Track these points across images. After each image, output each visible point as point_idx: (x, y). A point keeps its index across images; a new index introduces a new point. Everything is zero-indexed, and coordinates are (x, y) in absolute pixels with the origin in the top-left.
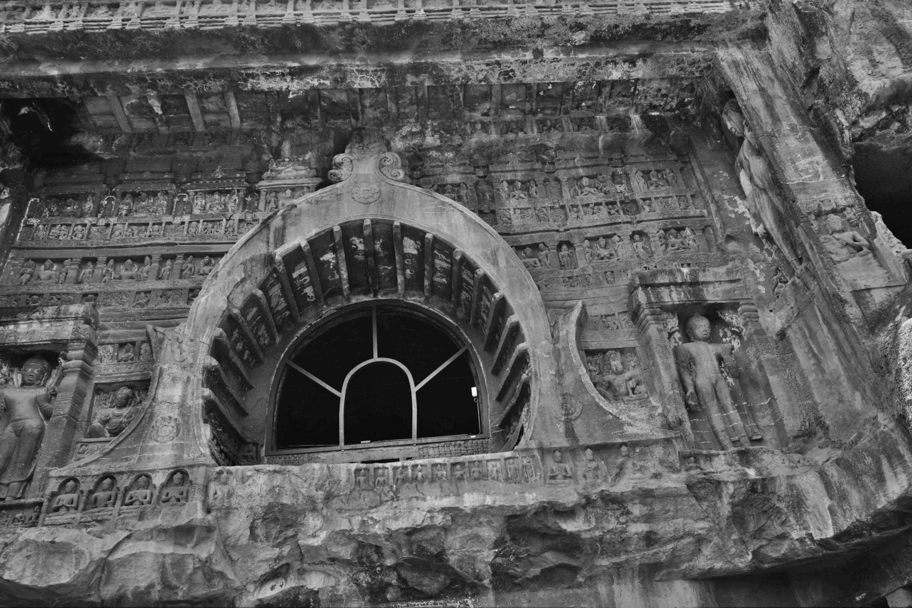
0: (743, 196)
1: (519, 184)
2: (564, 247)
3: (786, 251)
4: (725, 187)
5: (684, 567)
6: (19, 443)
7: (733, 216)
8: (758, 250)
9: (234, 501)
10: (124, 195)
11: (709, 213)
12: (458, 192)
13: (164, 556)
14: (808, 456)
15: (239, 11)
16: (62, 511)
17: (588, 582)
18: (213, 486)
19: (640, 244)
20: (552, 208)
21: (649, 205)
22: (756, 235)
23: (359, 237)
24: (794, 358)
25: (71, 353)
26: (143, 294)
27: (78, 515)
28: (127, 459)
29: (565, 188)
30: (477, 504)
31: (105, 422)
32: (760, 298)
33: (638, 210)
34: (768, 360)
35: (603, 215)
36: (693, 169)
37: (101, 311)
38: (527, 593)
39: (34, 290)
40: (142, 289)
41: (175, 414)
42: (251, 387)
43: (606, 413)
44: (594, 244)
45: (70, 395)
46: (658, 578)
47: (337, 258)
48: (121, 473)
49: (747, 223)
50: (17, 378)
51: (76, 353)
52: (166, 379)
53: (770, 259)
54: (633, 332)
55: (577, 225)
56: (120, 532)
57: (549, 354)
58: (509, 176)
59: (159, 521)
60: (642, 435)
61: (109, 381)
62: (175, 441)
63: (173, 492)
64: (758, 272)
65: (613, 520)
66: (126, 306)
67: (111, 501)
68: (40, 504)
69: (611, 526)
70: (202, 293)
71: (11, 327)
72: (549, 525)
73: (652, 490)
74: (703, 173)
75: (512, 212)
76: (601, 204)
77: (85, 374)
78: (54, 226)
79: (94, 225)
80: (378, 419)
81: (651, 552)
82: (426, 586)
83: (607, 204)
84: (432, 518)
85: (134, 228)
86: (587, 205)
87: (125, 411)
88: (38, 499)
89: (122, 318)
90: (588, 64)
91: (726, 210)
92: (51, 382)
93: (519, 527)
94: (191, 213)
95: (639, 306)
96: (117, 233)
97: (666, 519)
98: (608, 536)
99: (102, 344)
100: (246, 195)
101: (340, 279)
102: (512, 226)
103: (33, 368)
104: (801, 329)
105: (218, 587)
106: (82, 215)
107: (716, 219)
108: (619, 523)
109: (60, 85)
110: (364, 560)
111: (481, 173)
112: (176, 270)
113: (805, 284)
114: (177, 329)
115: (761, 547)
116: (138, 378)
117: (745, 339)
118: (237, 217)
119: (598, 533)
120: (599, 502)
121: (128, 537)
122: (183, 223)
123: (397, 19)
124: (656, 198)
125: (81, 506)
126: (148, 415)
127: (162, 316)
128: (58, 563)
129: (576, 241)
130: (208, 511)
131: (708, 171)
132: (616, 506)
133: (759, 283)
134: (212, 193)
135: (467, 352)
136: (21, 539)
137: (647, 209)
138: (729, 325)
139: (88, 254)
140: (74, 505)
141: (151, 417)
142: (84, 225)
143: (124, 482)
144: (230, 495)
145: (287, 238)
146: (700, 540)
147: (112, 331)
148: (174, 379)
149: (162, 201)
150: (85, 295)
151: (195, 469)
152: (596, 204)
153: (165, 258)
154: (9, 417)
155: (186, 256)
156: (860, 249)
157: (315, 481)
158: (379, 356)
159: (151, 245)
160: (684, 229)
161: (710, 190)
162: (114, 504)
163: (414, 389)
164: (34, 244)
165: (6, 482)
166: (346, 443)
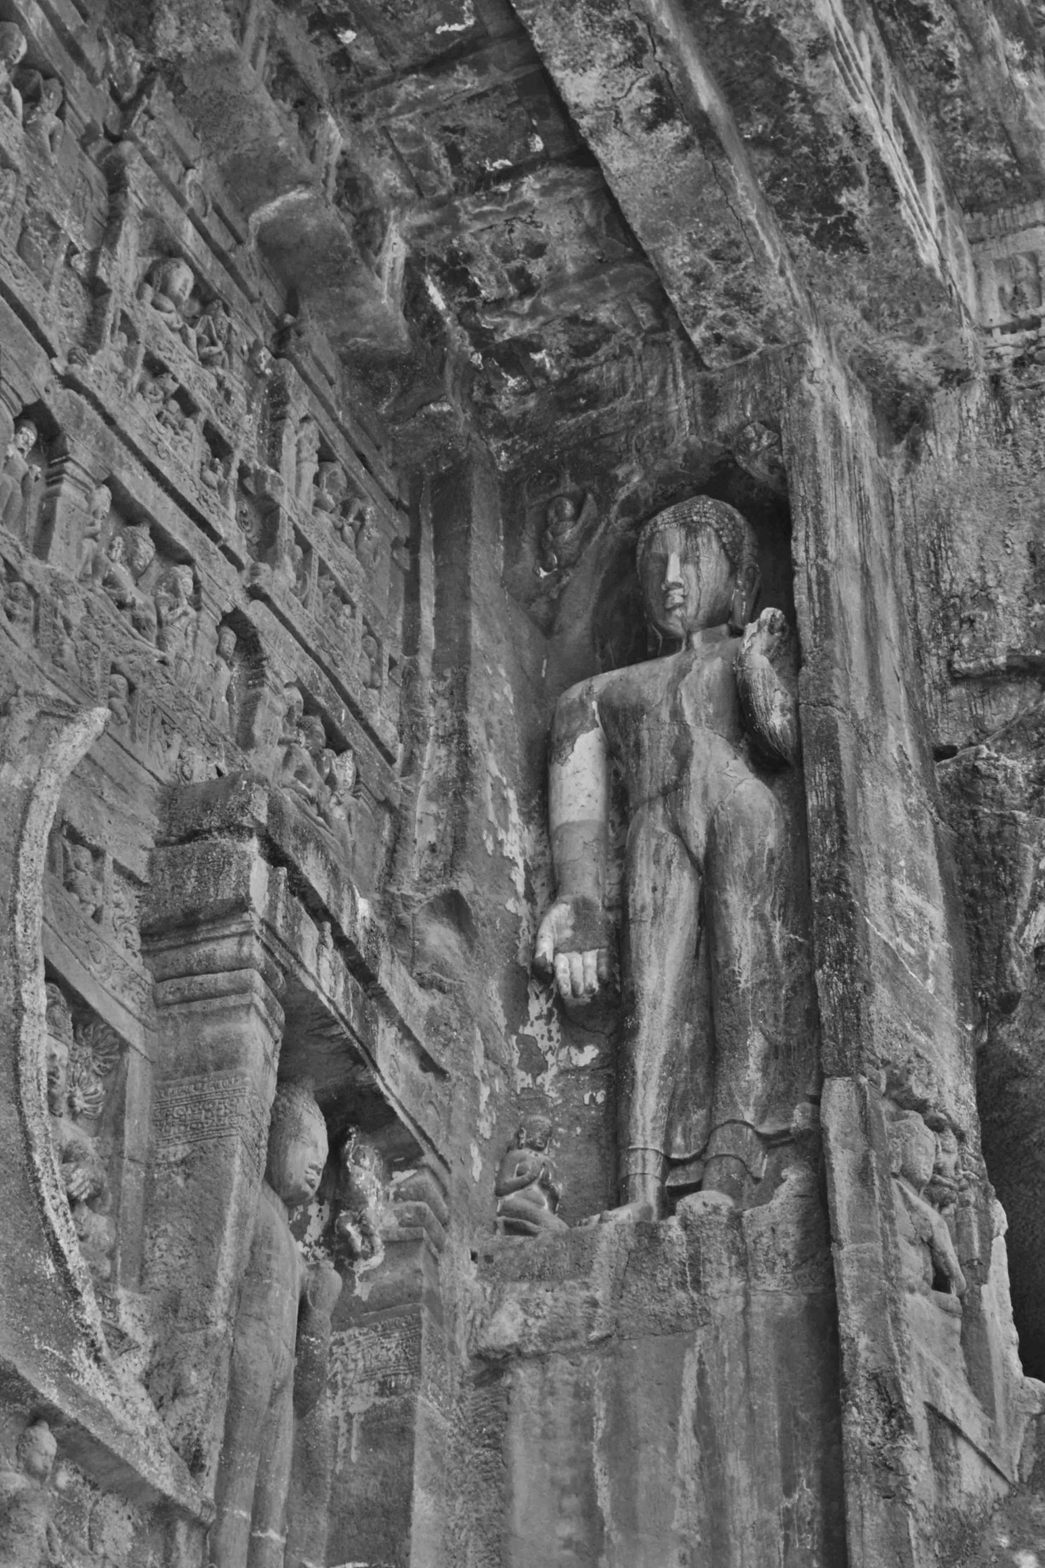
2: (29, 435)
7: (490, 846)
8: (502, 1021)
11: (410, 765)
19: (226, 674)
20: (72, 251)
22: (543, 975)
53: (523, 1079)
60: (119, 1430)
83: (211, 434)
91: (481, 805)
104: (582, 1393)
113: (696, 1261)
117: (362, 1291)
129: (81, 454)
152: (182, 396)
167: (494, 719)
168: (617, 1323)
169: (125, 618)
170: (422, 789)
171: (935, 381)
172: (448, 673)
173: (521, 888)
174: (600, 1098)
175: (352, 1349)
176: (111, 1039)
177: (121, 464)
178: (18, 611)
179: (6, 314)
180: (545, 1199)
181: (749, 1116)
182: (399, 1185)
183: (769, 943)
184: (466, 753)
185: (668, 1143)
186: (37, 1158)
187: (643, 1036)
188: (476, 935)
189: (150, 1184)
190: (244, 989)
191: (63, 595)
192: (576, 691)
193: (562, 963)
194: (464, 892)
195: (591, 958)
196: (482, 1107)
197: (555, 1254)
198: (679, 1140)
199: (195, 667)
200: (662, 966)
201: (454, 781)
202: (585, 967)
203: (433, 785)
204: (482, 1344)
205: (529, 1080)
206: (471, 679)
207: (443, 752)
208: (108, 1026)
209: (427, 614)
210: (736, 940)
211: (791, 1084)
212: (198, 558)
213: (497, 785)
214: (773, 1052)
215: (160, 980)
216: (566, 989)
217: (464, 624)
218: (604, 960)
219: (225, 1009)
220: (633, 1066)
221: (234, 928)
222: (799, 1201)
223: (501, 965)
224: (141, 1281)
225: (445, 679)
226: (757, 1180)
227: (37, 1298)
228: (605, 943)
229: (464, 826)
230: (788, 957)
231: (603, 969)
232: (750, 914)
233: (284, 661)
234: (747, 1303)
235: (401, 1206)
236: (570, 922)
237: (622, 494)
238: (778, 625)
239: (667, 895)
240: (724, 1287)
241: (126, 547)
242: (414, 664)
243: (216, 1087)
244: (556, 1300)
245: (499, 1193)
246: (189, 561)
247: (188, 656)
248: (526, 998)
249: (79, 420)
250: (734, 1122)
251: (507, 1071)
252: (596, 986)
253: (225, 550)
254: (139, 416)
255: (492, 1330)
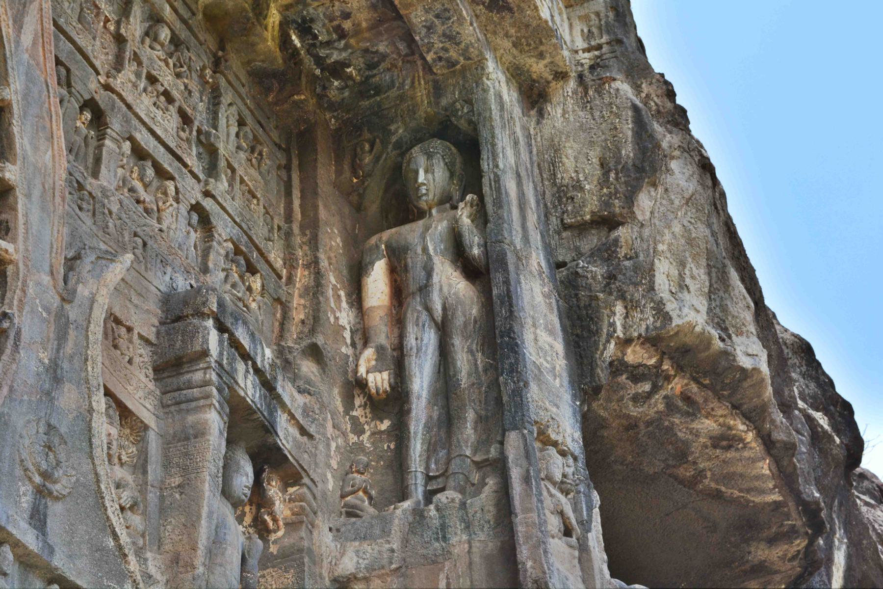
2: (88, 115)
7: (332, 320)
8: (341, 409)
11: (290, 280)
19: (194, 236)
20: (107, 20)
22: (361, 385)
54: (151, 393)
57: (47, 309)
83: (182, 113)
91: (327, 299)
113: (443, 527)
117: (273, 549)
129: (115, 125)
152: (166, 94)
167: (332, 255)
168: (404, 560)
169: (140, 208)
170: (297, 292)
171: (551, 77)
172: (308, 232)
173: (349, 341)
174: (392, 446)
175: (269, 579)
176: (139, 424)
177: (136, 129)
178: (85, 206)
179: (74, 53)
180: (366, 498)
181: (468, 453)
182: (291, 495)
183: (476, 364)
184: (318, 273)
185: (427, 468)
186: (103, 487)
187: (413, 414)
188: (326, 365)
189: (162, 498)
190: (208, 396)
191: (107, 197)
192: (374, 240)
193: (371, 378)
194: (319, 343)
195: (385, 375)
196: (332, 453)
197: (372, 526)
198: (433, 466)
199: (178, 232)
200: (421, 378)
201: (313, 287)
202: (383, 380)
203: (302, 290)
204: (336, 574)
205: (356, 438)
206: (320, 236)
207: (306, 273)
208: (138, 418)
209: (297, 203)
210: (459, 363)
211: (489, 435)
212: (177, 176)
213: (335, 289)
214: (479, 419)
215: (164, 393)
216: (373, 391)
217: (316, 207)
218: (392, 376)
219: (198, 407)
220: (408, 429)
221: (201, 366)
222: (495, 494)
223: (339, 380)
224: (159, 548)
225: (306, 235)
226: (473, 485)
227: (105, 558)
228: (392, 367)
229: (318, 310)
230: (485, 371)
231: (392, 380)
232: (466, 350)
233: (224, 229)
234: (470, 547)
235: (292, 505)
236: (374, 357)
237: (394, 139)
238: (475, 203)
239: (423, 343)
240: (458, 540)
241: (140, 172)
242: (291, 228)
243: (195, 447)
244: (373, 550)
245: (343, 497)
246: (172, 178)
247: (173, 227)
248: (353, 397)
249: (113, 107)
250: (461, 455)
251: (344, 434)
252: (388, 389)
253: (191, 172)
254: (144, 105)
255: (341, 566)
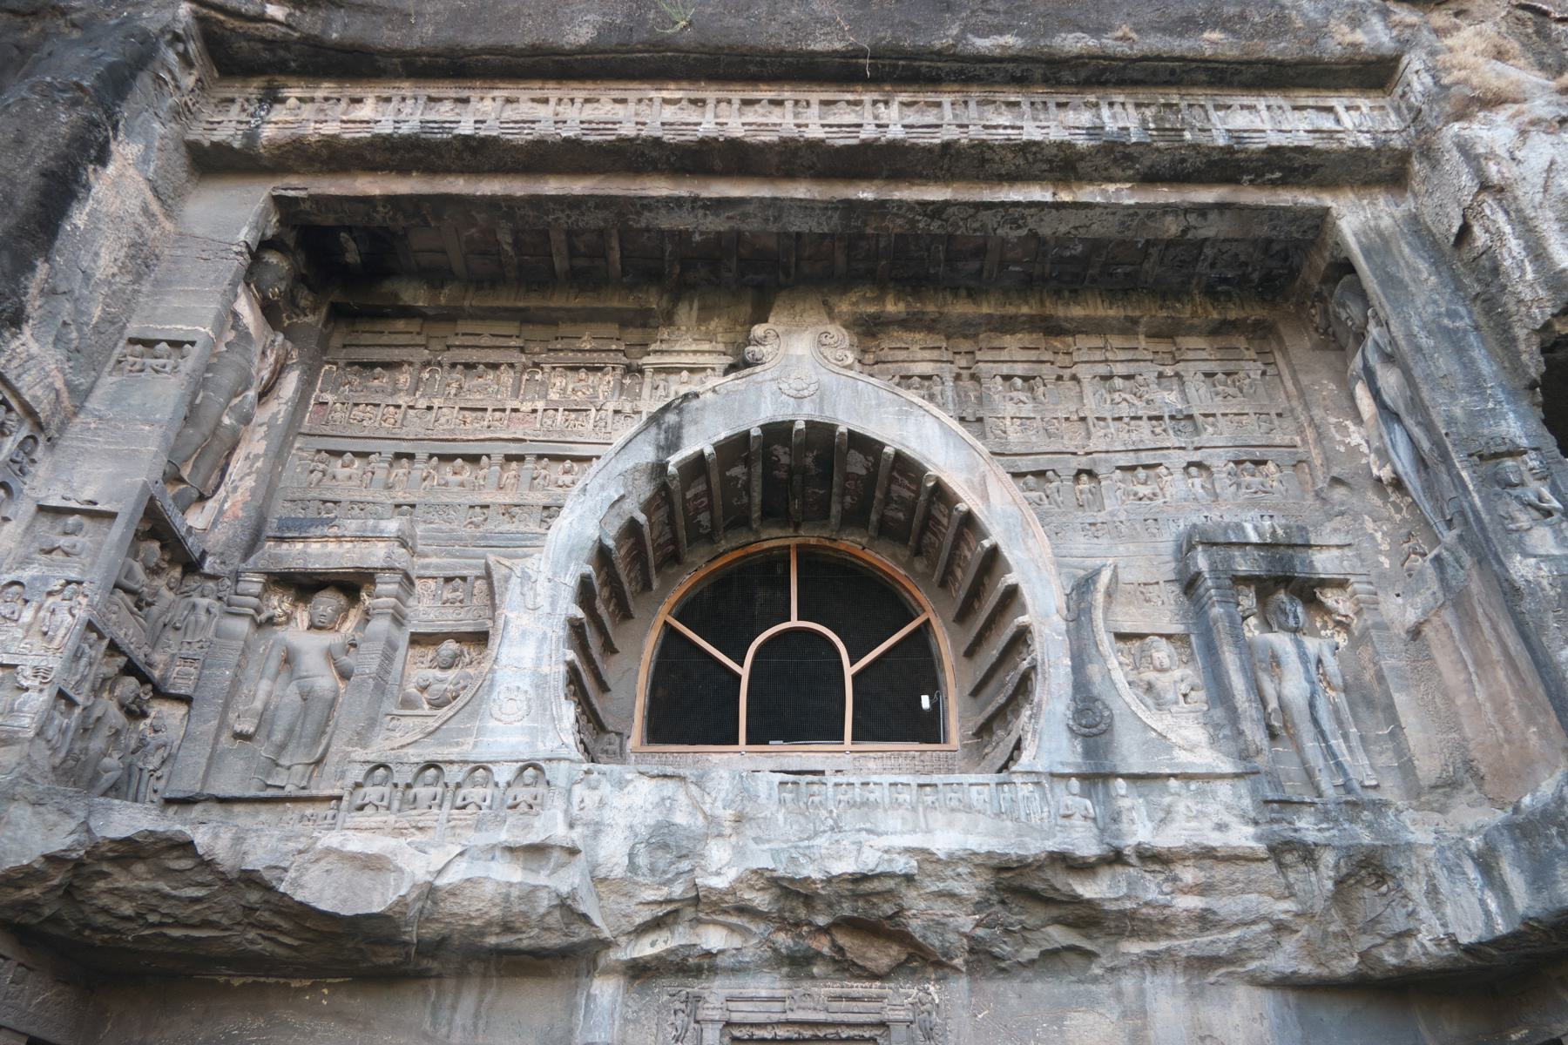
0: (1358, 418)
1: (1019, 382)
2: (1084, 478)
3: (1426, 506)
4: (1331, 405)
5: (1253, 965)
6: (305, 711)
7: (1342, 449)
8: (1379, 502)
9: (607, 815)
10: (453, 365)
11: (1304, 441)
12: (929, 388)
13: (511, 885)
14: (1450, 816)
15: (637, 114)
16: (369, 810)
17: (1108, 976)
18: (578, 791)
19: (1198, 481)
20: (1067, 419)
21: (1213, 425)
22: (1379, 480)
23: (785, 445)
24: (1434, 669)
25: (380, 587)
26: (478, 509)
27: (392, 818)
28: (457, 744)
29: (1088, 390)
30: (955, 847)
31: (423, 689)
32: (1382, 575)
33: (1197, 431)
34: (1392, 668)
35: (1144, 433)
36: (1279, 375)
37: (420, 530)
38: (1016, 983)
39: (328, 496)
40: (478, 502)
41: (525, 684)
42: (615, 651)
43: (1147, 727)
44: (1128, 475)
45: (380, 646)
46: (1212, 979)
47: (749, 474)
48: (452, 762)
49: (1364, 461)
50: (302, 616)
51: (387, 586)
52: (513, 632)
53: (1398, 517)
55: (1104, 448)
56: (449, 847)
58: (1005, 369)
59: (504, 836)
61: (429, 630)
62: (526, 723)
63: (524, 794)
64: (1379, 535)
65: (1153, 887)
66: (453, 526)
67: (436, 802)
68: (340, 798)
69: (1150, 897)
70: (564, 512)
71: (300, 546)
72: (1059, 886)
73: (1214, 849)
74: (1296, 382)
75: (1008, 421)
76: (1140, 418)
77: (398, 619)
78: (356, 405)
79: (411, 407)
80: (795, 709)
81: (1206, 939)
82: (872, 960)
83: (1150, 418)
84: (890, 861)
85: (467, 413)
86: (1120, 419)
87: (451, 674)
88: (336, 792)
89: (448, 542)
90: (1136, 214)
91: (1332, 439)
92: (349, 626)
93: (1016, 884)
94: (545, 397)
95: (1199, 574)
96: (443, 420)
97: (1231, 893)
98: (1144, 910)
99: (419, 577)
100: (623, 376)
101: (749, 506)
102: (1008, 443)
103: (327, 602)
105: (581, 934)
106: (395, 391)
107: (1314, 452)
108: (1162, 893)
109: (380, 209)
110: (787, 915)
111: (964, 363)
112: (525, 478)
113: (1457, 560)
114: (528, 562)
115: (1374, 946)
116: (470, 629)
118: (610, 406)
119: (1129, 905)
120: (1134, 860)
121: (461, 854)
122: (535, 411)
123: (862, 136)
124: (1224, 415)
125: (396, 805)
126: (487, 683)
127: (504, 543)
128: (367, 884)
129: (1101, 470)
130: (571, 826)
131: (1305, 380)
132: (1157, 868)
133: (1380, 552)
134: (576, 369)
135: (927, 622)
136: (319, 846)
137: (1210, 430)
138: (1328, 611)
139: (405, 447)
140: (385, 803)
141: (491, 685)
142: (398, 407)
143: (454, 774)
144: (602, 804)
145: (685, 441)
146: (1280, 928)
147: (434, 560)
148: (524, 634)
149: (507, 377)
150: (398, 506)
151: (554, 764)
152: (1133, 418)
153: (509, 458)
154: (292, 672)
155: (540, 457)
156: (1548, 513)
157: (723, 795)
158: (799, 619)
159: (490, 440)
160: (1264, 462)
161: (1307, 407)
162: (440, 806)
163: (849, 671)
164: (328, 430)
165: (287, 763)
166: (749, 742)
167: (1328, 402)
254: (1119, 437)
